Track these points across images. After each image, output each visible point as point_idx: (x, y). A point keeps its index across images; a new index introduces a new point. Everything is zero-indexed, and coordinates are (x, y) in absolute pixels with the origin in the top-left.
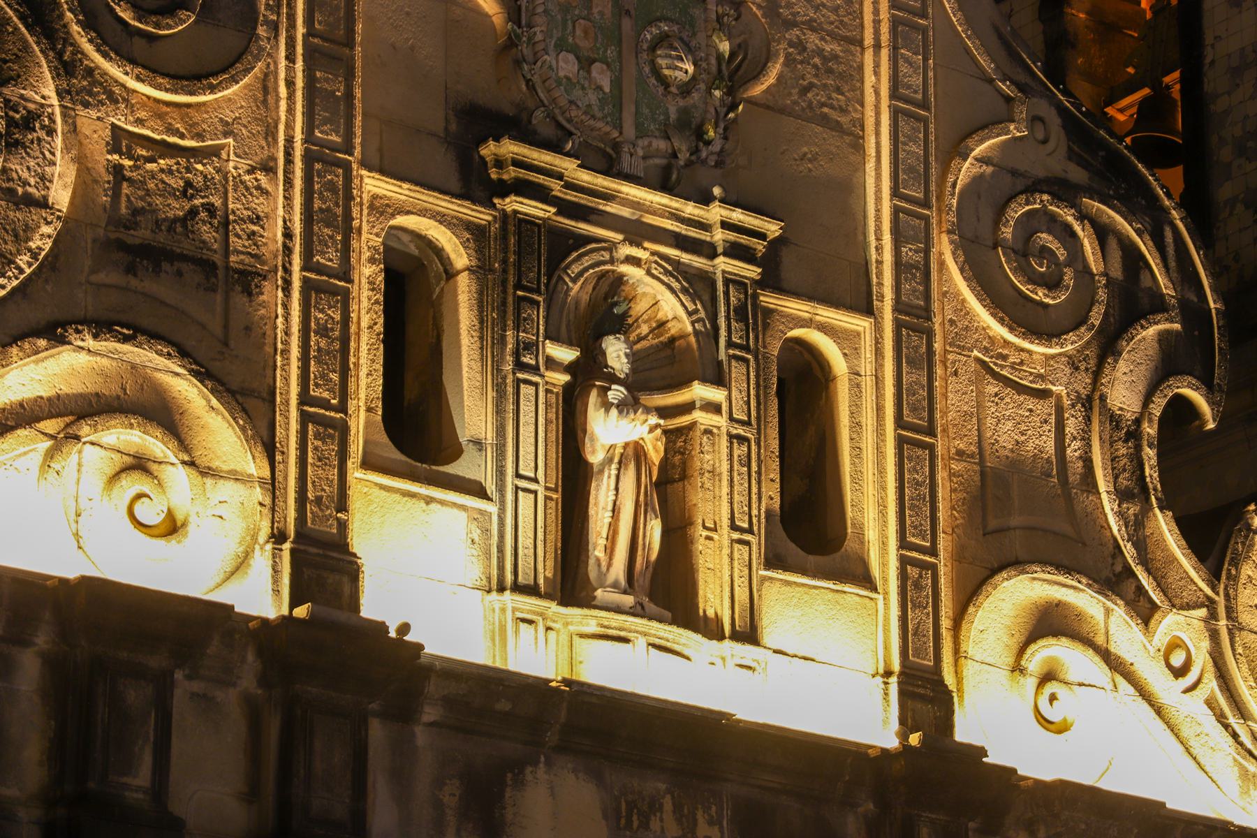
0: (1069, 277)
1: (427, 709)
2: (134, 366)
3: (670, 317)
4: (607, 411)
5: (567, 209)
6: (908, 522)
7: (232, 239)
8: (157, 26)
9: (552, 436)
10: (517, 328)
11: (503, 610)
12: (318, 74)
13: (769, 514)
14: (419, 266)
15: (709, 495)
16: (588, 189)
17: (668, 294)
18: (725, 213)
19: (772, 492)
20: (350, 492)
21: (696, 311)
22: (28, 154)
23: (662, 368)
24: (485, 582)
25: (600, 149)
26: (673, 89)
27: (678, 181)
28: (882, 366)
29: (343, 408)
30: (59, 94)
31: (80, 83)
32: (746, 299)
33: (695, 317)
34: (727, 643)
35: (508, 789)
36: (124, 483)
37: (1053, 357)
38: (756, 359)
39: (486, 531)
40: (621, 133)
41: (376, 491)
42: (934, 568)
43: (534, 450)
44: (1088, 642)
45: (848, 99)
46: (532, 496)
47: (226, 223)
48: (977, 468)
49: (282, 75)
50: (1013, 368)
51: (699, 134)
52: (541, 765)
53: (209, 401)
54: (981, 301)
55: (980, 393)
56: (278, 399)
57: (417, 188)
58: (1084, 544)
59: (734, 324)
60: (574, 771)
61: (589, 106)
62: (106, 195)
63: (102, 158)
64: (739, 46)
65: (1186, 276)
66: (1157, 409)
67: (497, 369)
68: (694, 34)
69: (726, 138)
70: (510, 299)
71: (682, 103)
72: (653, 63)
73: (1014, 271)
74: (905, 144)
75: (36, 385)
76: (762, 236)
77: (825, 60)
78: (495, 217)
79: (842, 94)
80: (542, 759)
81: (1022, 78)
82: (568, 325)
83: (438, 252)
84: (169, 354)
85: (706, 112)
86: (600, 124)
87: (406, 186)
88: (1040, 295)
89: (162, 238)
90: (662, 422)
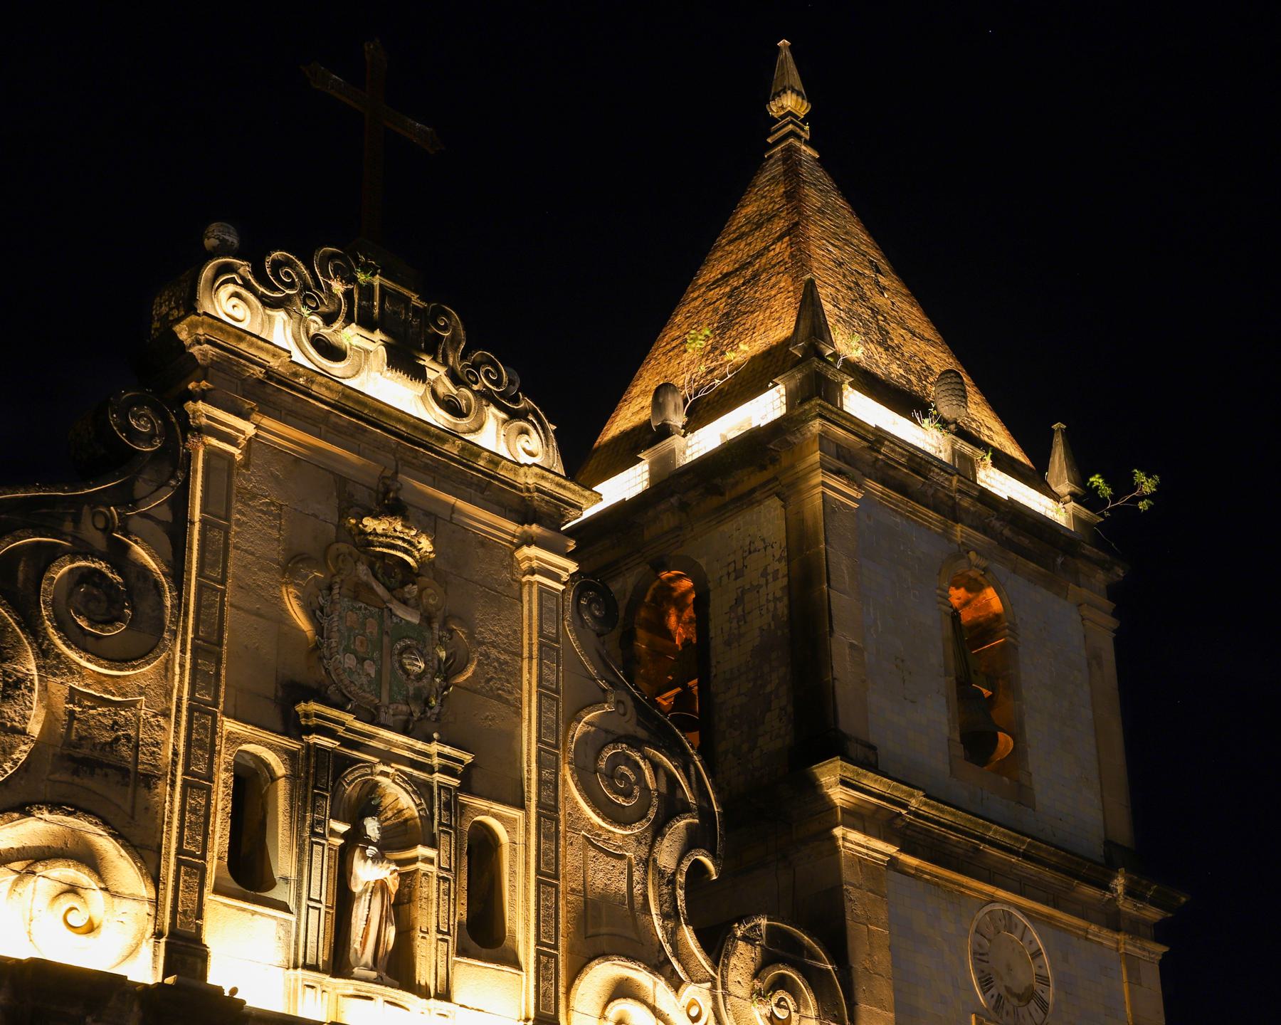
2: (73, 830)
7: (140, 755)
27: (413, 729)
42: (556, 957)
44: (644, 1002)
47: (137, 746)
49: (177, 661)
51: (427, 702)
55: (585, 856)
63: (62, 706)
71: (417, 685)
76: (461, 762)
83: (267, 766)
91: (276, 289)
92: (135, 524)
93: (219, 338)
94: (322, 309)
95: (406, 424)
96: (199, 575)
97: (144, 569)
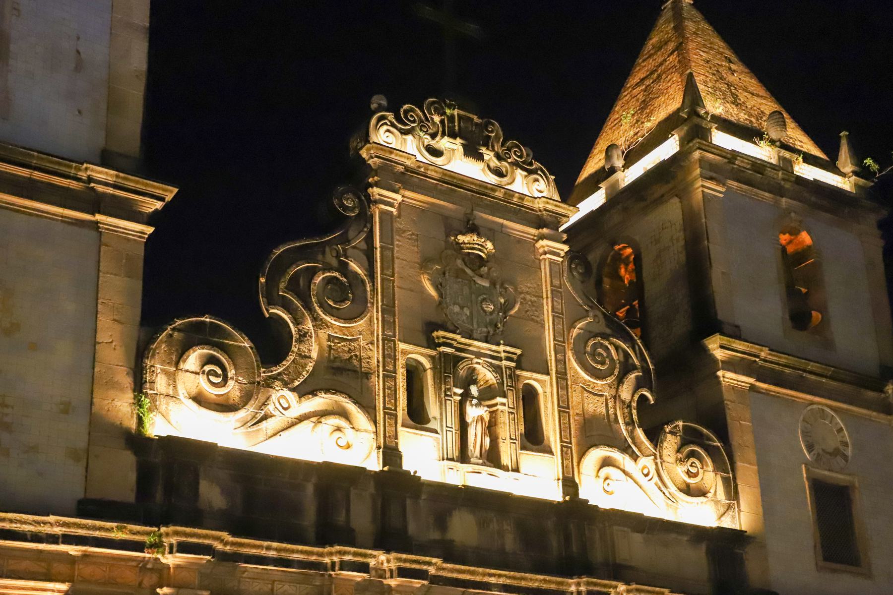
0: (607, 361)
5: (458, 349)
13: (521, 434)
14: (416, 368)
19: (522, 428)
23: (488, 394)
42: (571, 448)
43: (452, 420)
44: (618, 468)
47: (361, 359)
51: (496, 326)
55: (583, 396)
63: (325, 343)
66: (636, 397)
71: (491, 317)
76: (515, 354)
88: (599, 367)
91: (406, 125)
92: (349, 252)
93: (381, 154)
94: (430, 131)
95: (475, 185)
96: (382, 273)
97: (356, 273)
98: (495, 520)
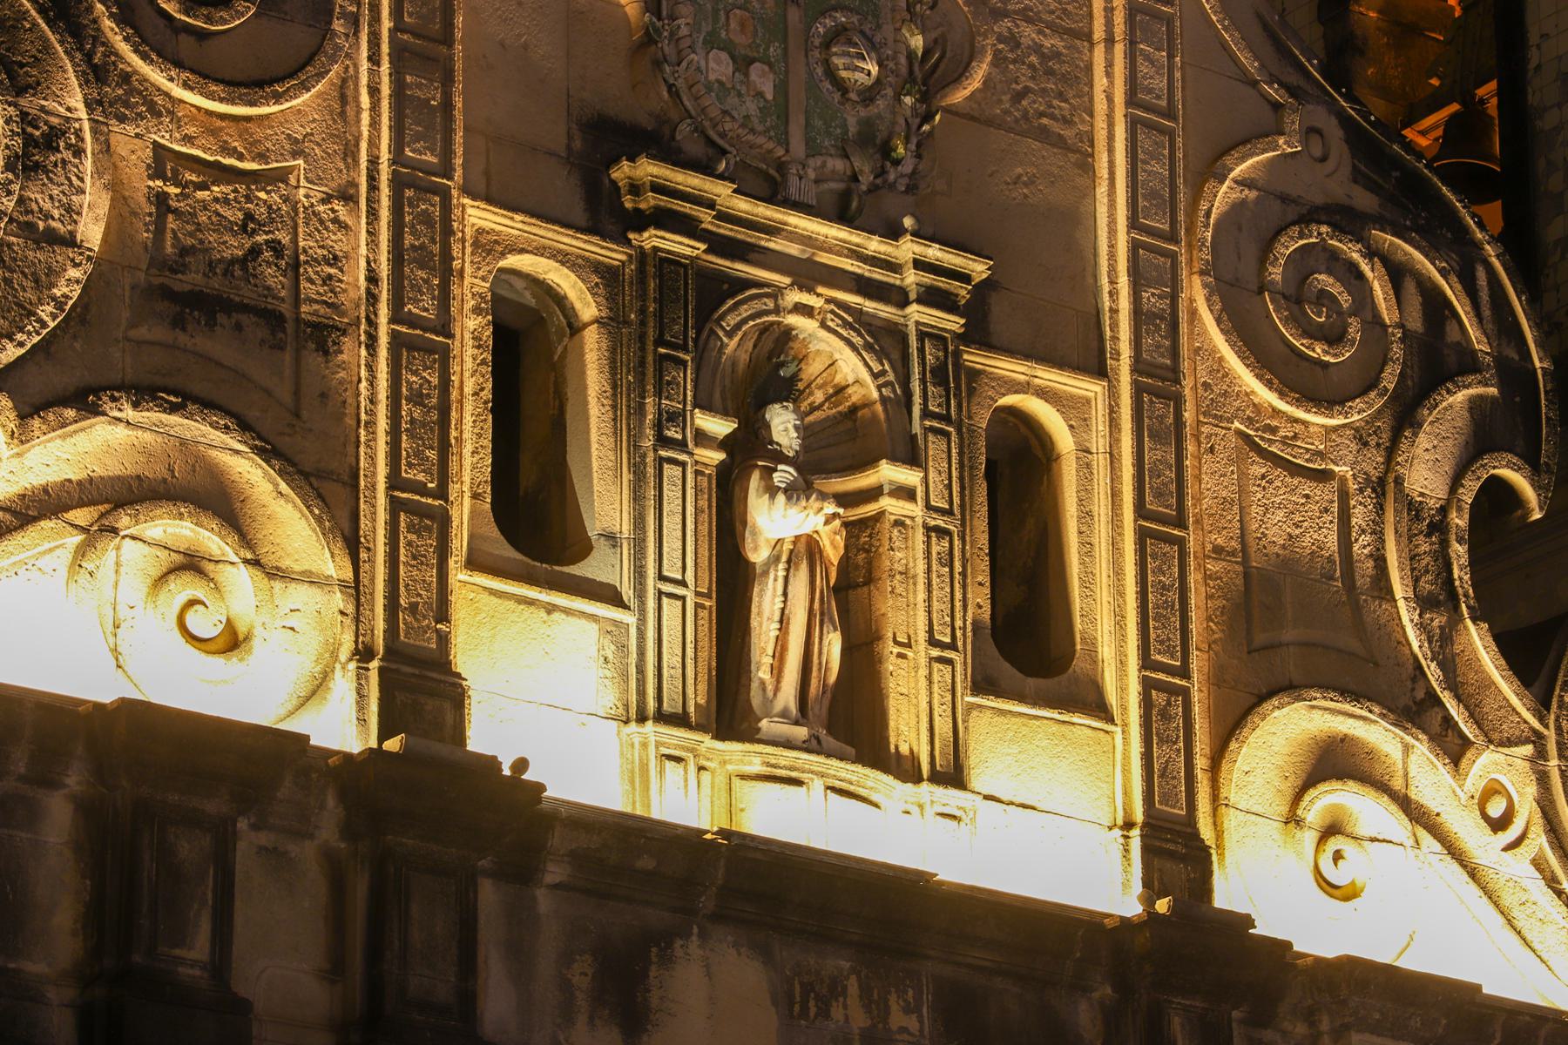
0: (1354, 329)
1: (551, 867)
2: (183, 443)
3: (851, 381)
4: (773, 497)
5: (720, 246)
6: (1152, 636)
7: (303, 284)
8: (209, 20)
9: (704, 529)
10: (659, 394)
11: (644, 745)
12: (408, 79)
13: (974, 623)
14: (538, 319)
15: (901, 602)
16: (746, 220)
17: (847, 351)
18: (918, 249)
19: (980, 598)
20: (453, 598)
21: (883, 373)
22: (51, 180)
23: (840, 446)
24: (621, 711)
25: (761, 171)
26: (853, 96)
27: (860, 210)
28: (1118, 440)
29: (442, 493)
30: (88, 105)
31: (114, 91)
32: (946, 357)
33: (881, 380)
34: (925, 787)
35: (653, 968)
36: (172, 586)
37: (1335, 429)
38: (959, 432)
39: (622, 647)
40: (787, 151)
41: (485, 597)
42: (1185, 693)
44: (1383, 787)
45: (1074, 108)
46: (679, 603)
47: (296, 265)
48: (1239, 568)
49: (364, 80)
50: (1284, 443)
51: (886, 150)
52: (694, 938)
53: (276, 485)
54: (1243, 359)
55: (1243, 475)
56: (362, 483)
57: (533, 221)
58: (1376, 664)
59: (930, 388)
60: (736, 945)
61: (747, 117)
62: (147, 231)
63: (141, 184)
64: (936, 41)
65: (1504, 328)
66: (1468, 494)
67: (634, 446)
68: (879, 27)
69: (919, 156)
70: (650, 358)
71: (863, 113)
72: (827, 63)
73: (1285, 321)
74: (1145, 162)
75: (64, 466)
76: (964, 278)
77: (1044, 57)
78: (630, 256)
79: (1066, 101)
80: (695, 930)
81: (1294, 79)
82: (723, 392)
83: (560, 300)
84: (226, 427)
85: (894, 123)
86: (761, 140)
87: (518, 217)
88: (1318, 351)
89: (216, 283)
90: (841, 511)
98: (853, 986)
